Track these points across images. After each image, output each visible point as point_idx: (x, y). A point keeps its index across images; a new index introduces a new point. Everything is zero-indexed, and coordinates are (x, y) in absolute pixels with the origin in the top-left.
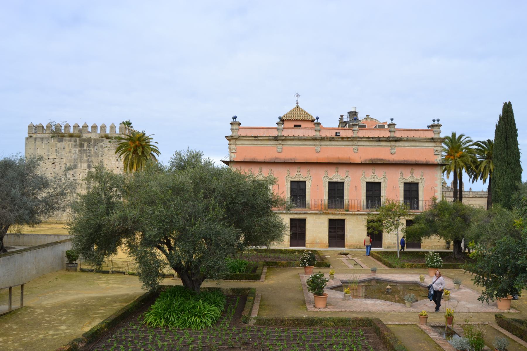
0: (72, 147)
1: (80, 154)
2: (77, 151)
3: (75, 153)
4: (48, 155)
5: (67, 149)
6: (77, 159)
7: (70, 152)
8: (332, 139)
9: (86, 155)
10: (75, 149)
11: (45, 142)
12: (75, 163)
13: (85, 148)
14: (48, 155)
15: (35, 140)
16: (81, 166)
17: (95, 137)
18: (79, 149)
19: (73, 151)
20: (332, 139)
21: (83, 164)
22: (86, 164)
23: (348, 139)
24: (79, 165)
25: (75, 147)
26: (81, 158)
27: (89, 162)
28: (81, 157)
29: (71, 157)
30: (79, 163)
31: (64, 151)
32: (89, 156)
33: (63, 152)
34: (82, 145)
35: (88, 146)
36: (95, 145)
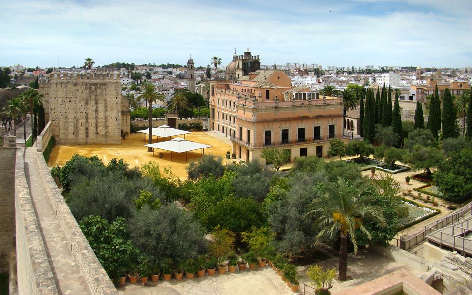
2: (87, 93)
4: (66, 95)
5: (80, 91)
7: (83, 93)
11: (63, 85)
13: (93, 90)
14: (66, 95)
15: (57, 84)
16: (91, 103)
19: (84, 92)
21: (92, 102)
25: (86, 89)
27: (96, 100)
28: (90, 96)
32: (97, 96)
33: (78, 93)
34: (91, 88)
35: (96, 89)
36: (100, 88)
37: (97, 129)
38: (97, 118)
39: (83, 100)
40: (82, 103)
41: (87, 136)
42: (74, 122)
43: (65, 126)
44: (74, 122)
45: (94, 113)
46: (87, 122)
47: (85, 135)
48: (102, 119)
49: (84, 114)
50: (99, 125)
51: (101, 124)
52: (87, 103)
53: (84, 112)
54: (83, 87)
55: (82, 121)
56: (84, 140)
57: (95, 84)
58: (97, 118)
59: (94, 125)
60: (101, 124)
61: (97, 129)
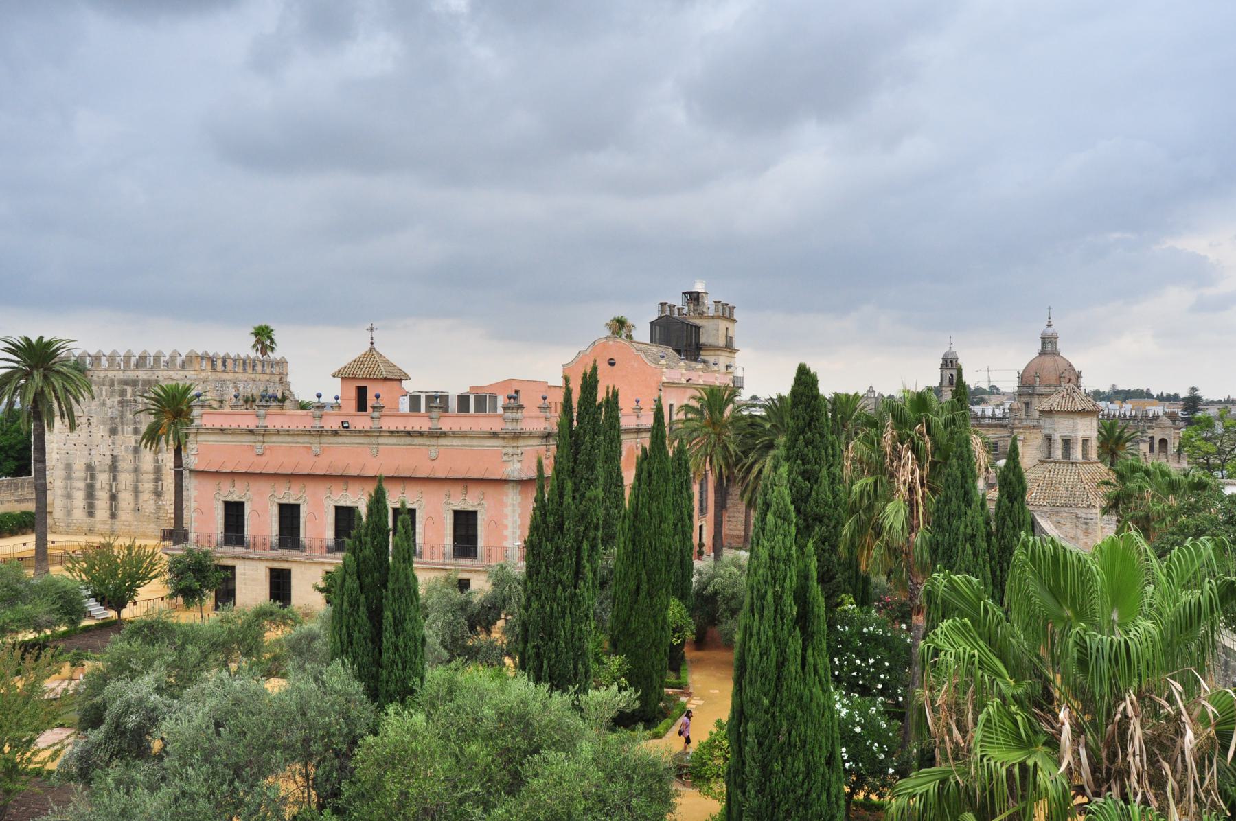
0: (106, 396)
1: (120, 409)
2: (116, 404)
3: (113, 406)
6: (116, 418)
8: (335, 433)
9: (130, 410)
10: (112, 399)
12: (113, 425)
17: (145, 377)
18: (119, 399)
19: (109, 402)
20: (335, 433)
22: (132, 427)
23: (365, 434)
24: (119, 429)
26: (122, 415)
28: (122, 414)
29: (106, 414)
30: (119, 425)
31: (94, 403)
34: (123, 393)
37: (136, 497)
38: (136, 470)
39: (104, 423)
40: (103, 430)
41: (113, 516)
42: (86, 479)
43: (66, 488)
44: (86, 479)
45: (131, 457)
46: (115, 479)
47: (109, 512)
48: (147, 473)
49: (108, 460)
50: (141, 488)
51: (146, 485)
52: (113, 432)
53: (108, 453)
54: (104, 388)
55: (103, 478)
56: (108, 527)
57: (134, 383)
58: (136, 470)
59: (130, 488)
60: (146, 485)
61: (136, 497)
